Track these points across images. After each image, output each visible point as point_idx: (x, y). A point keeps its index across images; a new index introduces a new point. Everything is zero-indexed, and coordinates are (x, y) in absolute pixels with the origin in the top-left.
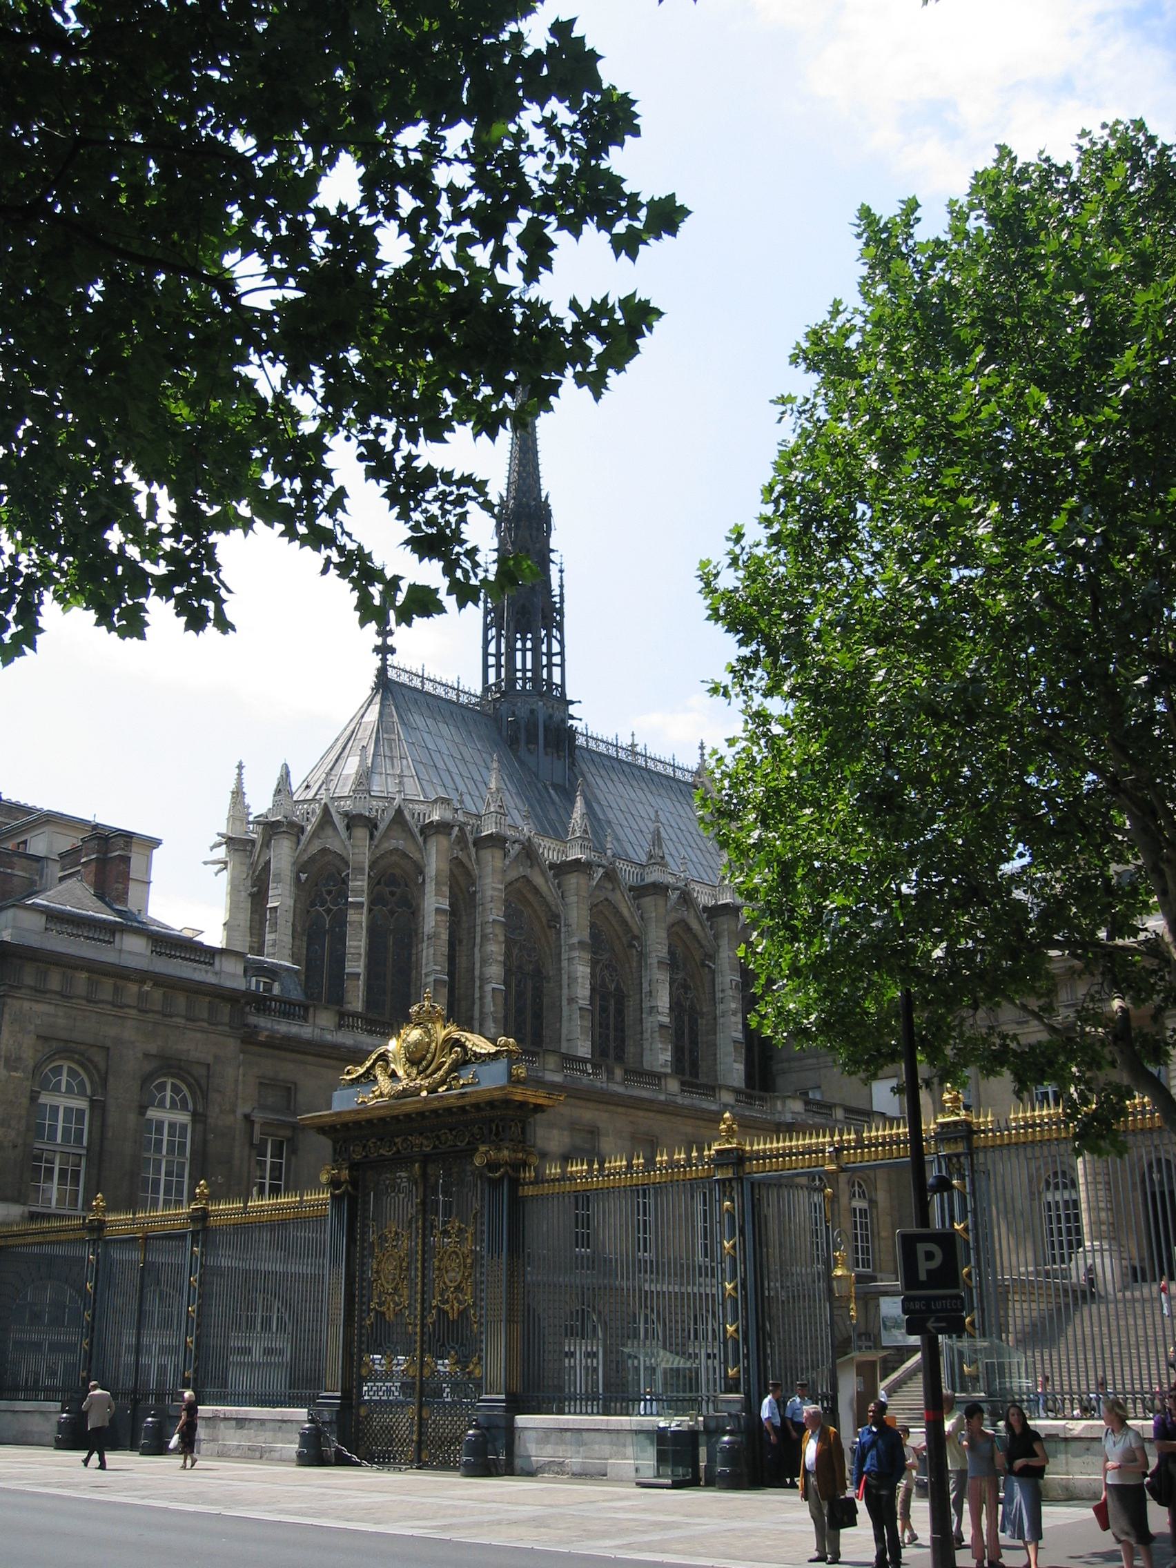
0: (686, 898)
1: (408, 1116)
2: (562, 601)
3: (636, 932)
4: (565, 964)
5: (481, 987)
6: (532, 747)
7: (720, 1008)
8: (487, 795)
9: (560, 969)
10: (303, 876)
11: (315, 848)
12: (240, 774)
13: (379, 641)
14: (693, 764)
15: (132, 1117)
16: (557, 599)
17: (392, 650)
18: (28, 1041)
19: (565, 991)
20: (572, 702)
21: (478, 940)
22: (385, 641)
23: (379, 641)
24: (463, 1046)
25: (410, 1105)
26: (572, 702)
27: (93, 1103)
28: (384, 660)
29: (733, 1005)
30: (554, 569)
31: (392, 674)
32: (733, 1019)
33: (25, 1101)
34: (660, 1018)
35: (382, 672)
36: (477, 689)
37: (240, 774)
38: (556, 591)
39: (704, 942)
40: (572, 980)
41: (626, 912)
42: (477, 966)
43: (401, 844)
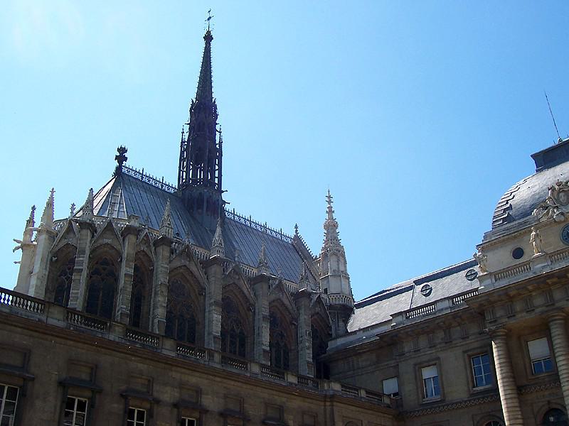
0: (280, 287)
2: (220, 146)
3: (252, 302)
4: (207, 314)
5: (153, 321)
6: (200, 211)
7: (300, 346)
8: (167, 223)
10: (54, 259)
11: (61, 245)
12: (33, 212)
14: (292, 234)
16: (217, 146)
17: (126, 159)
19: (207, 328)
21: (153, 295)
23: (118, 154)
29: (307, 344)
31: (124, 170)
32: (308, 351)
34: (264, 347)
35: (119, 169)
36: (175, 184)
37: (33, 212)
38: (217, 142)
39: (292, 312)
40: (211, 321)
41: (246, 291)
42: (152, 309)
43: (109, 241)
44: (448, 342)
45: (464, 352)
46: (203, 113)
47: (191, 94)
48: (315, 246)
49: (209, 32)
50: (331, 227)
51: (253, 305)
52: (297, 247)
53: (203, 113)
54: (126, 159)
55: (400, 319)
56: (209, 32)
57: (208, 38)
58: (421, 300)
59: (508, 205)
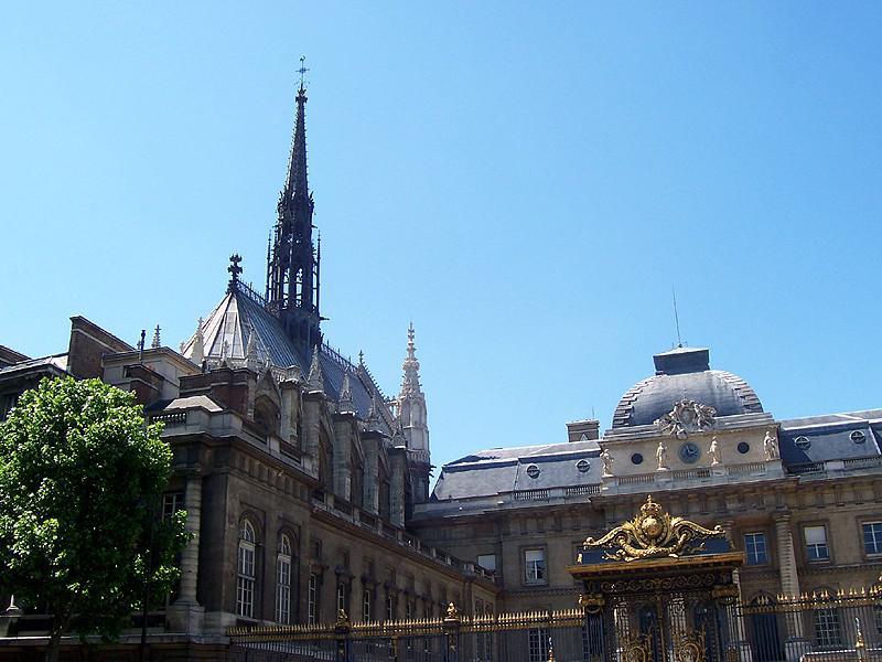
1: (661, 569)
2: (319, 258)
9: (332, 478)
12: (157, 334)
13: (233, 263)
15: (274, 558)
18: (237, 505)
20: (323, 319)
22: (236, 264)
24: (690, 529)
25: (663, 562)
26: (323, 319)
27: (257, 547)
28: (234, 276)
30: (314, 237)
33: (235, 544)
43: (267, 393)
44: (558, 530)
45: (574, 543)
46: (296, 209)
47: (280, 180)
48: (390, 385)
49: (302, 92)
50: (412, 370)
51: (363, 463)
52: (363, 381)
53: (296, 209)
54: (241, 270)
55: (508, 498)
56: (302, 92)
57: (301, 100)
58: (527, 483)
59: (630, 407)
